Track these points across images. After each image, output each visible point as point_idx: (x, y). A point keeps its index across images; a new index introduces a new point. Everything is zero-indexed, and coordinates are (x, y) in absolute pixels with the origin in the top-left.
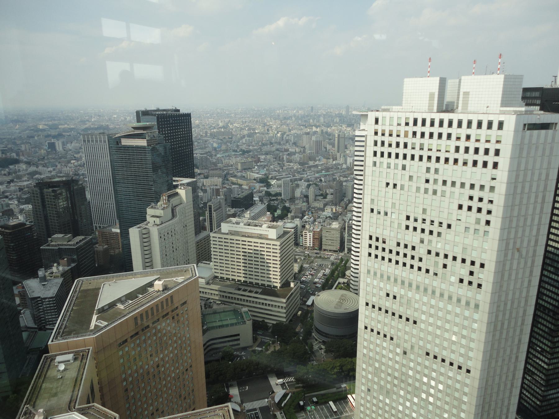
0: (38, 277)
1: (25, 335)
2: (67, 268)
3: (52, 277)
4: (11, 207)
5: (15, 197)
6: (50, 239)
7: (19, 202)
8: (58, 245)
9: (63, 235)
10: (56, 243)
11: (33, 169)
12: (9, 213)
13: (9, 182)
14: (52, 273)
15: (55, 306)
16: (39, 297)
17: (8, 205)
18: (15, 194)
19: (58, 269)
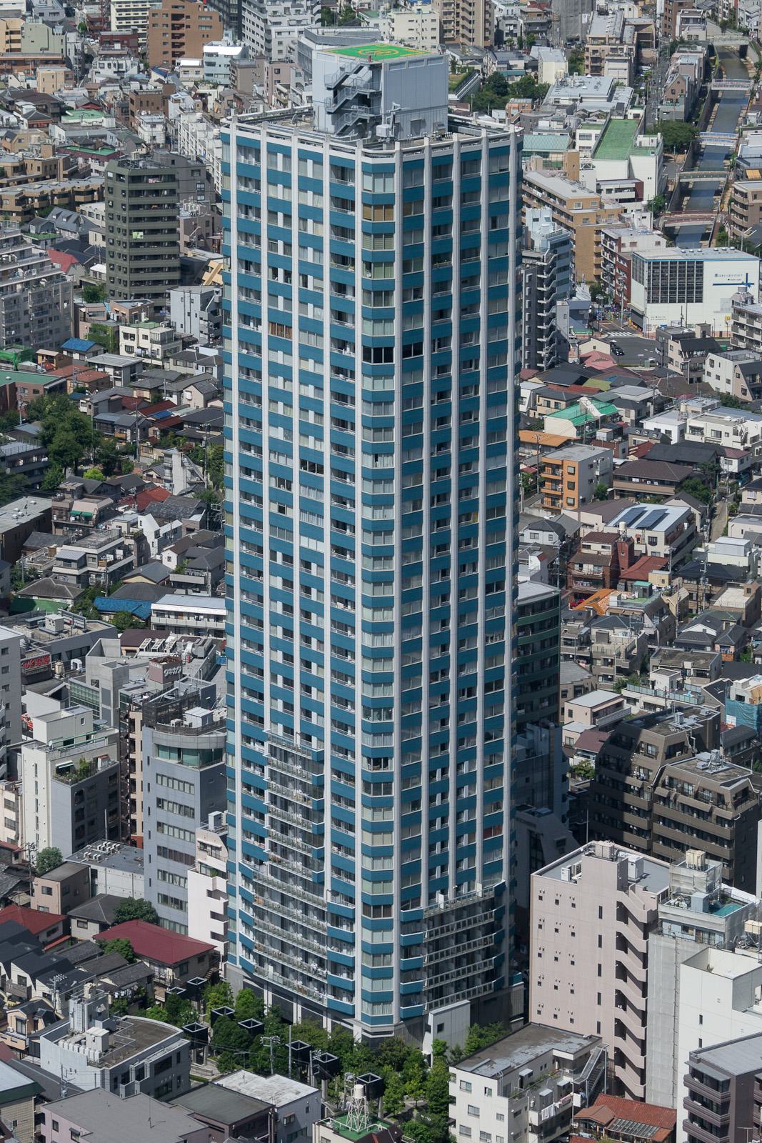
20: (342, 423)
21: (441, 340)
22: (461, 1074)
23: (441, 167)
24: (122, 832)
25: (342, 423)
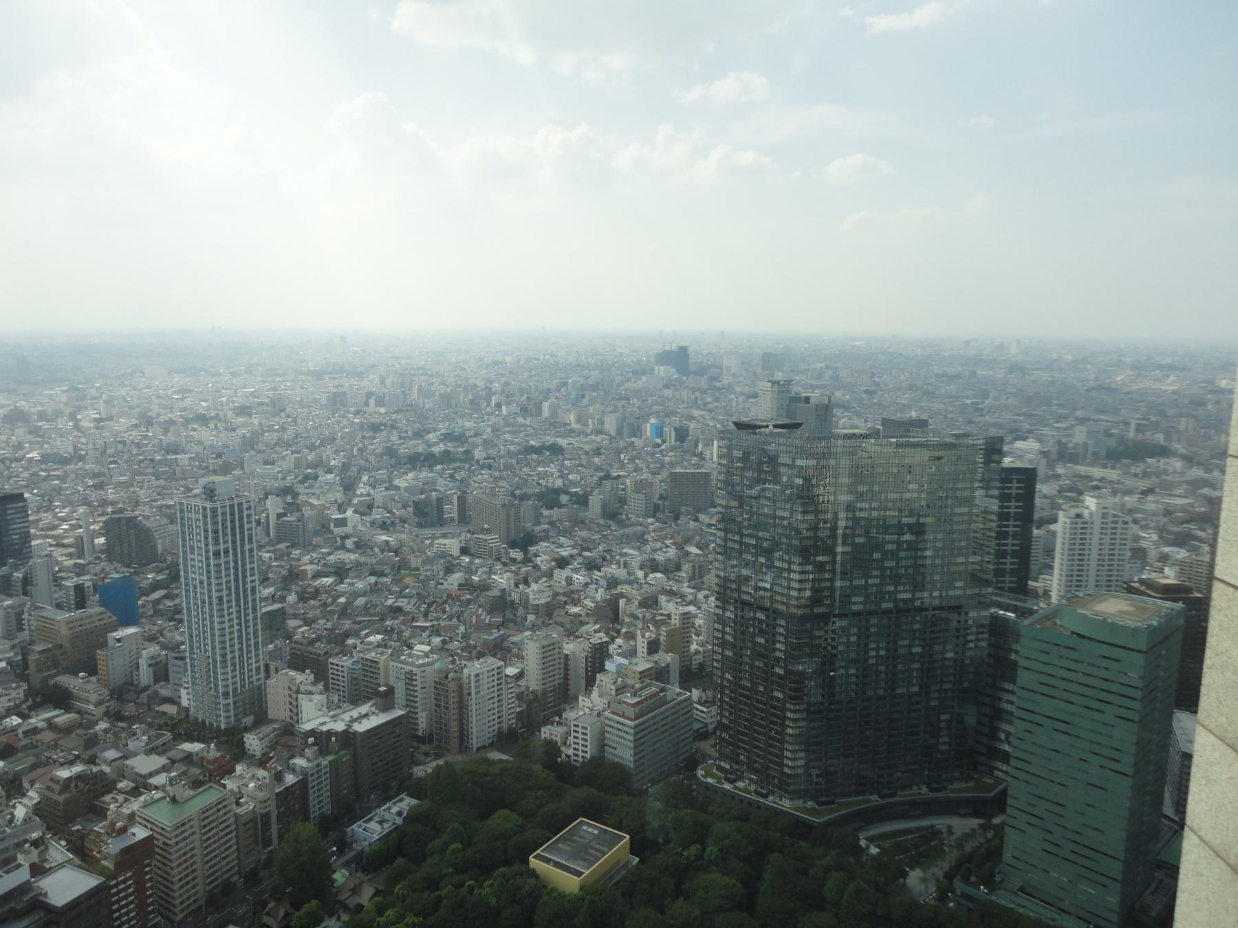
4: (1143, 544)
5: (1153, 525)
7: (1161, 537)
11: (1196, 473)
12: (1140, 554)
13: (1145, 493)
17: (1137, 539)
18: (1155, 518)
20: (208, 572)
21: (235, 549)
22: (246, 735)
23: (232, 507)
24: (167, 679)
25: (208, 572)
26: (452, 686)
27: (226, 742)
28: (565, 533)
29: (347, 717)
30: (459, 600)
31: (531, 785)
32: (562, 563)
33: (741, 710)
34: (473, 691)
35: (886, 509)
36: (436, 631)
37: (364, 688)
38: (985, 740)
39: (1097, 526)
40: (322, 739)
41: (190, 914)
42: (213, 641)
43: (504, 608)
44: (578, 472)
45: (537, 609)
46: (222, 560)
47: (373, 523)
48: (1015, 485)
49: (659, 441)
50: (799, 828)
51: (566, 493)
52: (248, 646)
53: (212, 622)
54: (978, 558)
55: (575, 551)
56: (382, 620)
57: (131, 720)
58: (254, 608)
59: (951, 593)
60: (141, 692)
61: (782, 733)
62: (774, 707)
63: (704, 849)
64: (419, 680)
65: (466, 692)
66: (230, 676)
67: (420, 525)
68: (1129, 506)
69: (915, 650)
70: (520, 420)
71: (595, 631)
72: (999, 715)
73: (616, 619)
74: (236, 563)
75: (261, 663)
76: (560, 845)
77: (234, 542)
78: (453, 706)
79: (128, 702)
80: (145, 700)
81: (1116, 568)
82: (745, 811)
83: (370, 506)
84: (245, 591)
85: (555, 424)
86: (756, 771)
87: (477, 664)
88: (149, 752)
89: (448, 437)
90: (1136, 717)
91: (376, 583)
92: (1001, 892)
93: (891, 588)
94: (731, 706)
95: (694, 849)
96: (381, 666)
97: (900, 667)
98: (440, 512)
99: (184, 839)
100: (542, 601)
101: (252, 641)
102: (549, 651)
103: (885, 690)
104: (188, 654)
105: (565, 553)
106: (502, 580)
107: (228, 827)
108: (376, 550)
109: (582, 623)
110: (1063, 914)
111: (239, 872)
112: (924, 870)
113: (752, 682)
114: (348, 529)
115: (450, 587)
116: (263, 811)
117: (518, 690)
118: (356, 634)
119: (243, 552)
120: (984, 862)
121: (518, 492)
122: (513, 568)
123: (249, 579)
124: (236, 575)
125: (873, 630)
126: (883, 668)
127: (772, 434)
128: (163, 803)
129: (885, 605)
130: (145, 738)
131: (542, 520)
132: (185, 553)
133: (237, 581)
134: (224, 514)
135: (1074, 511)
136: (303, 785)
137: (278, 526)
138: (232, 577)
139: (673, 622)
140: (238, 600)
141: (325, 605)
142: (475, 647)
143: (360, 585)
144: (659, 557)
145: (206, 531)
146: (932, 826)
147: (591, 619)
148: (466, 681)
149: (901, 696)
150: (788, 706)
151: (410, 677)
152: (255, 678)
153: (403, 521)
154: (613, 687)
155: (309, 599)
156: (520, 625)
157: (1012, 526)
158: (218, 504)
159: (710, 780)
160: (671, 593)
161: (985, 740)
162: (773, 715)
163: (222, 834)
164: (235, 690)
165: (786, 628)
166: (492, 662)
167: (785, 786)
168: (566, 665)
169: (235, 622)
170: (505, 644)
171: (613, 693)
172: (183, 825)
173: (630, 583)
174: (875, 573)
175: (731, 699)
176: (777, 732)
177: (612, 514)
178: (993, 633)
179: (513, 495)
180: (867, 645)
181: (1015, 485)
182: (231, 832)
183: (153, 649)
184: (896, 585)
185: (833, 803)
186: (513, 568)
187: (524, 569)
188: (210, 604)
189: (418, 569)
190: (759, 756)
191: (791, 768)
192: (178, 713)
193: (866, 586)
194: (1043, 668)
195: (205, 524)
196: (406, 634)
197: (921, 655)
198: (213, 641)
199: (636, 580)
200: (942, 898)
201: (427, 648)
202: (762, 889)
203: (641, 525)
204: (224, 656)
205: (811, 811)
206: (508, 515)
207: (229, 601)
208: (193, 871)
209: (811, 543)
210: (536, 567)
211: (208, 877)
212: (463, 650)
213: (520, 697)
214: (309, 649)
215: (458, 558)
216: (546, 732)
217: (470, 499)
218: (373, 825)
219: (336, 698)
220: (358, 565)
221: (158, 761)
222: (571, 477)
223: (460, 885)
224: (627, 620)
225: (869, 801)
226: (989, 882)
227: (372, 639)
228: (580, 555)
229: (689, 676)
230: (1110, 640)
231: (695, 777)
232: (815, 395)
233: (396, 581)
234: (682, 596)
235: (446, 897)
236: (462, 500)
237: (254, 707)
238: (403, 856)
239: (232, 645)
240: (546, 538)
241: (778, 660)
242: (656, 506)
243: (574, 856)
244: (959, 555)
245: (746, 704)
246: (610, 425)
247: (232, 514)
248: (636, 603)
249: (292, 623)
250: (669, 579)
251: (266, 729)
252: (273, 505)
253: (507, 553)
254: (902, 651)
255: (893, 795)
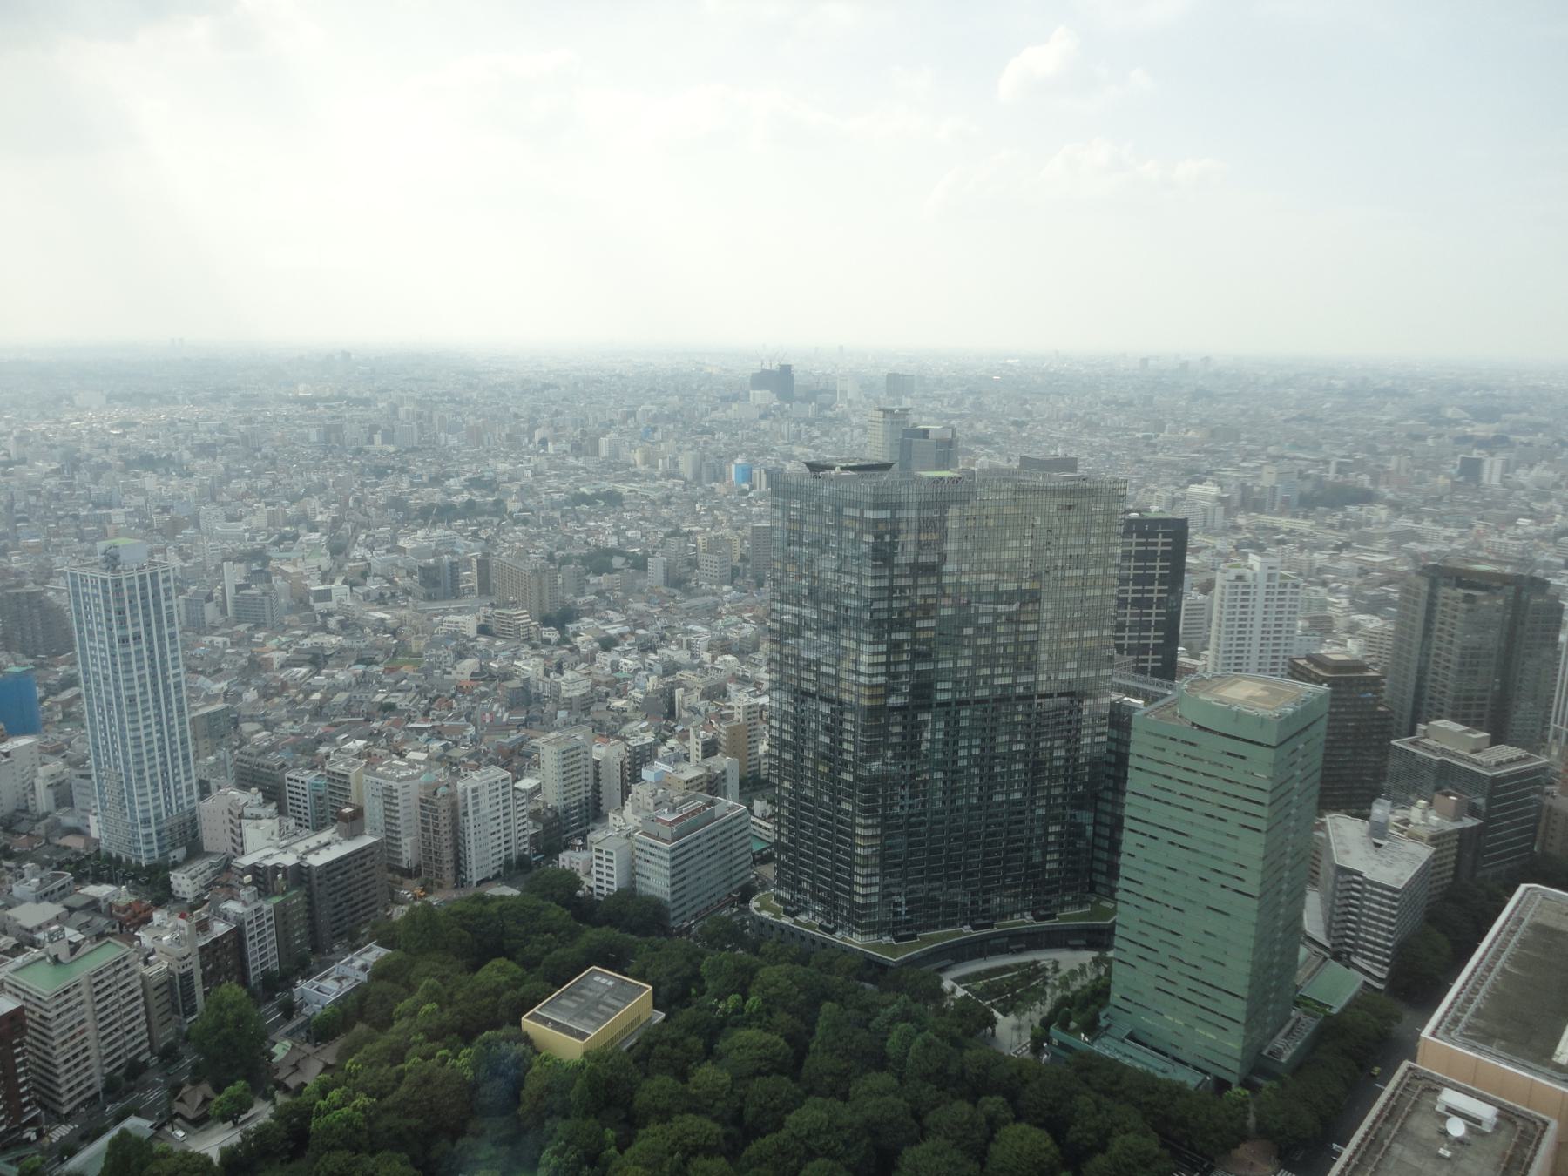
0: (1366, 817)
1: (1303, 952)
2: (1450, 826)
3: (1402, 831)
4: (1330, 611)
5: (1345, 587)
6: (1421, 727)
7: (1352, 603)
8: (1443, 751)
9: (1460, 728)
10: (1439, 745)
11: (1404, 522)
12: (1322, 626)
13: (1339, 548)
14: (1406, 822)
15: (1393, 916)
16: (1359, 874)
17: (1324, 605)
19: (1425, 819)
20: (114, 664)
21: (149, 634)
23: (142, 578)
24: (72, 804)
25: (114, 664)
26: (443, 805)
27: (148, 882)
28: (613, 605)
29: (301, 847)
30: (470, 694)
31: (546, 924)
32: (607, 644)
33: (803, 827)
34: (470, 810)
35: (979, 572)
36: (437, 734)
37: (334, 810)
38: (1105, 856)
39: (1262, 590)
40: (263, 878)
41: (82, 1104)
42: (125, 754)
43: (529, 703)
44: (639, 527)
45: (569, 704)
46: (132, 649)
47: (367, 596)
48: (1160, 540)
49: (746, 487)
50: (873, 969)
51: (621, 553)
52: (174, 759)
53: (122, 729)
54: (1095, 633)
55: (627, 629)
56: (368, 720)
57: (21, 857)
58: (181, 710)
59: (1062, 676)
60: (38, 821)
61: (852, 854)
62: (842, 822)
63: (745, 999)
64: (401, 798)
65: (461, 811)
66: (150, 797)
67: (429, 598)
68: (1317, 565)
69: (1017, 747)
70: (571, 460)
71: (643, 730)
72: (1117, 825)
73: (671, 714)
74: (151, 651)
75: (194, 781)
76: (563, 1002)
77: (148, 625)
78: (445, 829)
79: (20, 834)
80: (42, 832)
81: (1282, 641)
82: (804, 952)
83: (364, 575)
84: (167, 687)
85: (615, 465)
86: (822, 901)
87: (475, 775)
88: (44, 896)
89: (475, 483)
90: (1262, 825)
91: (364, 674)
92: (1105, 1040)
93: (987, 672)
94: (791, 822)
95: (733, 999)
96: (352, 780)
97: (997, 769)
98: (455, 580)
99: (69, 1010)
100: (577, 693)
101: (180, 753)
102: (572, 757)
103: (980, 799)
104: (93, 771)
105: (613, 631)
106: (529, 666)
107: (132, 992)
108: (368, 630)
109: (626, 720)
110: (1177, 1065)
111: (150, 1048)
112: (1018, 1017)
113: (815, 790)
114: (332, 605)
115: (460, 677)
116: (182, 971)
117: (533, 807)
118: (331, 740)
119: (161, 638)
120: (1088, 1006)
121: (558, 554)
122: (545, 651)
123: (171, 672)
124: (153, 667)
125: (963, 723)
126: (976, 771)
127: (838, 477)
128: (40, 967)
129: (978, 693)
130: (36, 880)
131: (587, 589)
132: (82, 639)
133: (154, 675)
134: (131, 588)
135: (1233, 573)
136: (238, 935)
137: (236, 601)
138: (147, 671)
139: (736, 717)
140: (157, 701)
141: (294, 702)
142: (486, 753)
143: (341, 676)
144: (733, 635)
145: (108, 611)
146: (1035, 962)
147: (639, 715)
148: (460, 797)
149: (1001, 804)
150: (858, 820)
151: (389, 795)
152: (185, 800)
153: (408, 592)
154: (651, 801)
155: (273, 695)
156: (547, 724)
157: (1156, 591)
158: (123, 576)
159: (766, 914)
160: (743, 680)
161: (1105, 856)
162: (840, 831)
163: (123, 1002)
164: (158, 816)
165: (854, 724)
166: (497, 773)
167: (858, 918)
168: (597, 773)
169: (154, 728)
170: (525, 748)
171: (651, 807)
172: (66, 992)
173: (692, 668)
174: (966, 652)
175: (792, 813)
176: (846, 853)
177: (677, 581)
178: (1112, 725)
179: (551, 558)
180: (956, 743)
181: (1160, 540)
182: (136, 998)
183: (56, 765)
184: (992, 667)
185: (914, 937)
186: (545, 651)
187: (559, 652)
188: (119, 705)
189: (420, 655)
190: (824, 882)
191: (863, 896)
192: (87, 848)
193: (955, 670)
194: (1158, 768)
195: (107, 601)
196: (397, 738)
197: (1026, 753)
198: (125, 754)
199: (701, 665)
200: (1036, 1049)
201: (422, 756)
202: (813, 1046)
203: (714, 594)
204: (140, 772)
205: (889, 949)
206: (540, 583)
207: (145, 701)
208: (85, 1050)
209: (884, 616)
210: (574, 650)
211: (107, 1056)
212: (470, 757)
213: (535, 815)
214: (260, 760)
215: (474, 640)
216: (566, 859)
217: (494, 562)
218: (330, 984)
219: (292, 823)
220: (341, 652)
221: (52, 910)
222: (629, 534)
223: (428, 1057)
224: (685, 715)
225: (960, 934)
226: (1092, 1028)
227: (350, 745)
228: (632, 633)
229: (752, 785)
230: (1236, 735)
231: (748, 910)
232: (935, 427)
233: (389, 671)
234: (757, 684)
235: (410, 1071)
236: (483, 564)
237: (189, 839)
238: (365, 1021)
239: (151, 759)
240: (591, 611)
241: (845, 764)
242: (735, 571)
243: (580, 1015)
244: (1073, 629)
245: (808, 819)
246: (685, 466)
247: (143, 588)
248: (697, 694)
249: (247, 727)
250: (742, 663)
251: (201, 865)
252: (234, 574)
253: (538, 632)
254: (1001, 750)
255: (990, 926)
